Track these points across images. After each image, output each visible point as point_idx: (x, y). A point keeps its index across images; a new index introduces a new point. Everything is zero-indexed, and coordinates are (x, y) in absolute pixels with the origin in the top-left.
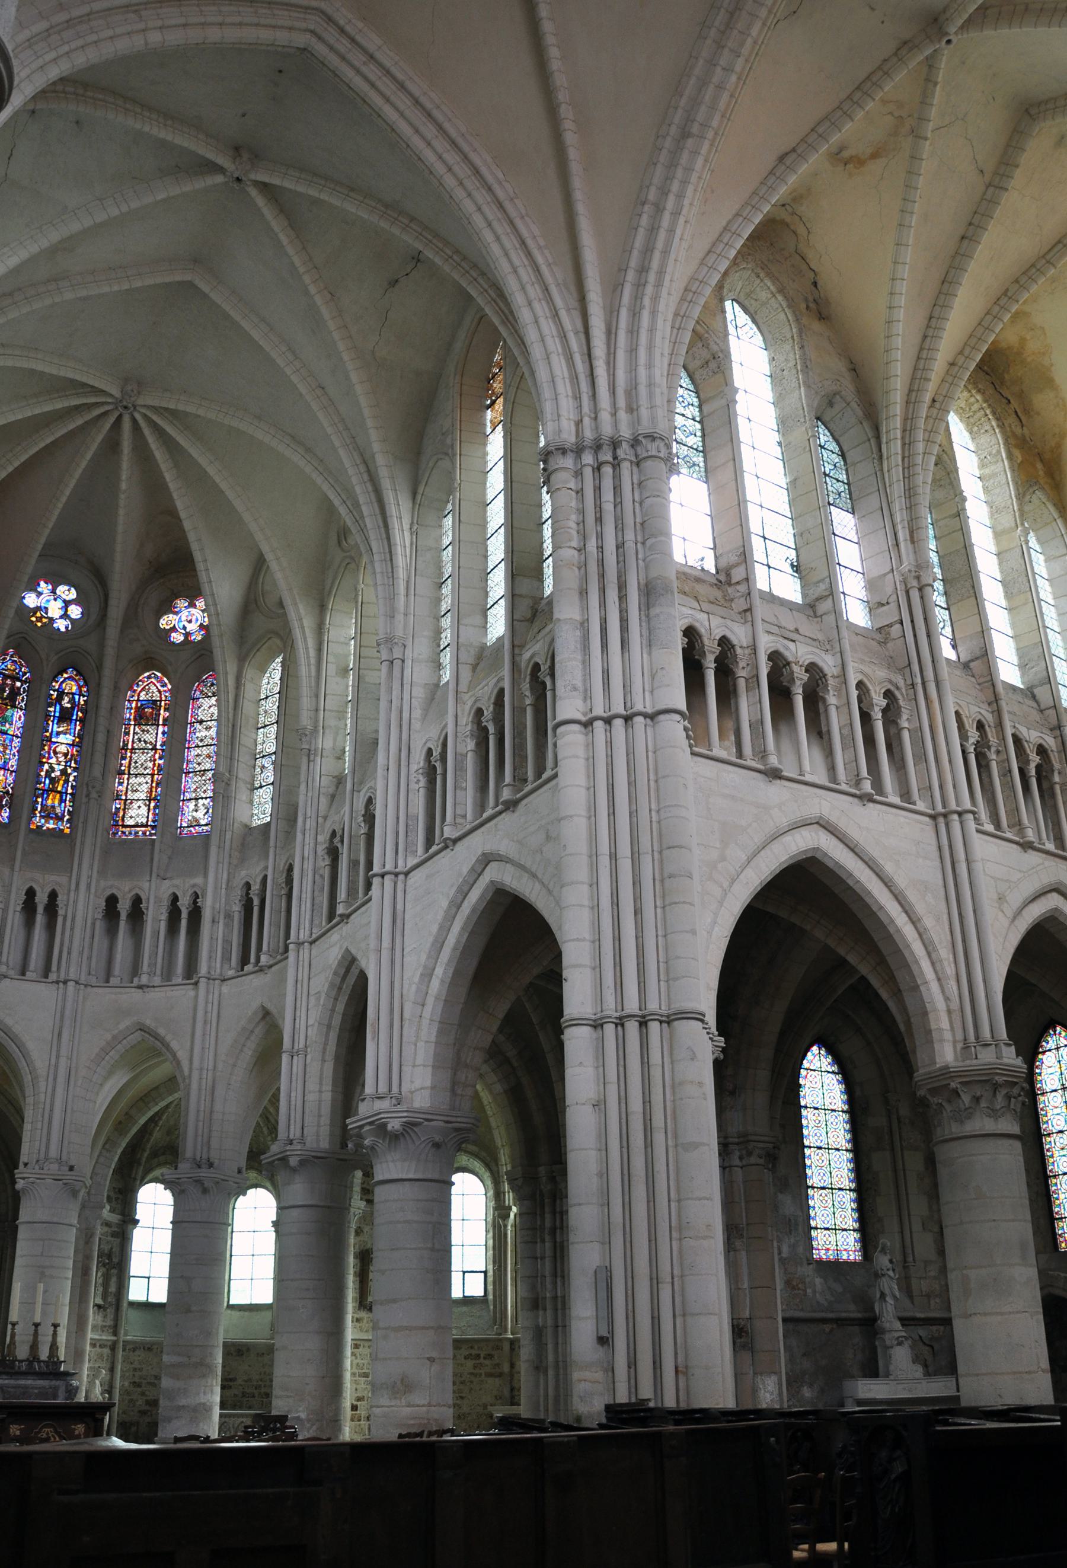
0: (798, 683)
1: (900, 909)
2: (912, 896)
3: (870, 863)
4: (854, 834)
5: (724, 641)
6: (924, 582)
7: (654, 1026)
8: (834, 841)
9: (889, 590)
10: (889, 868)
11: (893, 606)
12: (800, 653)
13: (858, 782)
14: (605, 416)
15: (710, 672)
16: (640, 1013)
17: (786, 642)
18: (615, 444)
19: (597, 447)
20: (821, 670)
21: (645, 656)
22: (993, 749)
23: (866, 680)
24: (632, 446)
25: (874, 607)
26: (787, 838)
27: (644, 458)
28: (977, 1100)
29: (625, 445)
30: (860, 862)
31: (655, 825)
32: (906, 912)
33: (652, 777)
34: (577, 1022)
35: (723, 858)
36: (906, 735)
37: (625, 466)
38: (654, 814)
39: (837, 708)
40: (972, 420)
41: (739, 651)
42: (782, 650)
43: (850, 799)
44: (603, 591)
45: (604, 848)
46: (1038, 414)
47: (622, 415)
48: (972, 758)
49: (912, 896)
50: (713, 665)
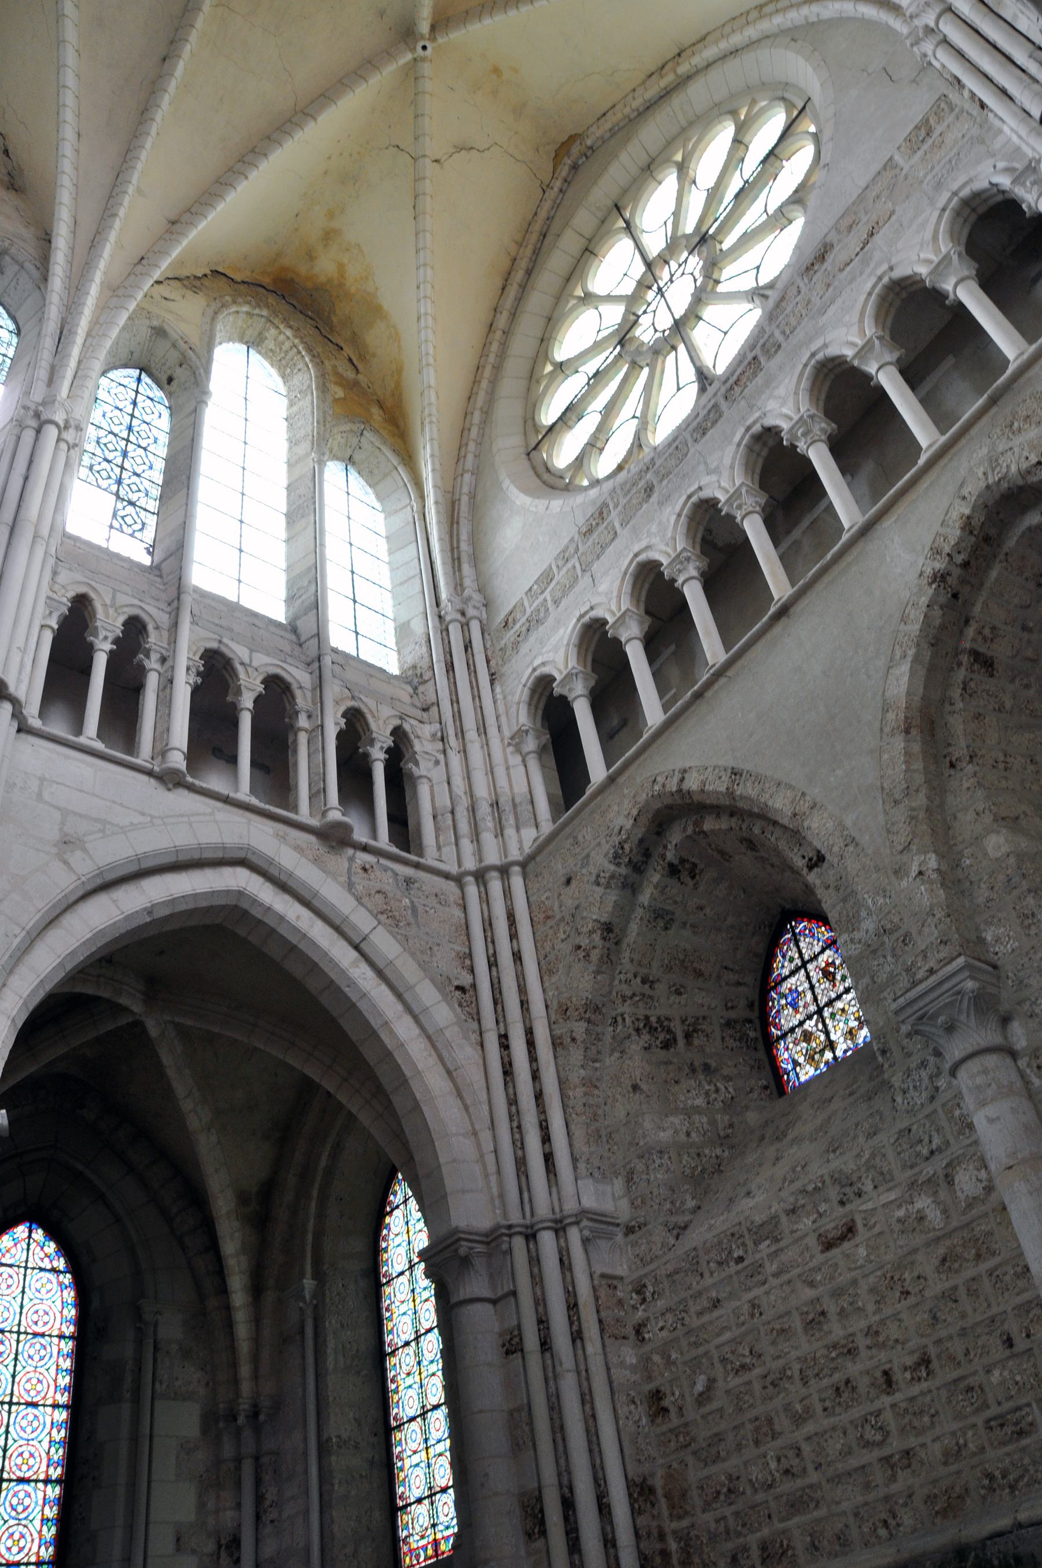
6: (44, 417)
40: (284, 362)
46: (374, 355)
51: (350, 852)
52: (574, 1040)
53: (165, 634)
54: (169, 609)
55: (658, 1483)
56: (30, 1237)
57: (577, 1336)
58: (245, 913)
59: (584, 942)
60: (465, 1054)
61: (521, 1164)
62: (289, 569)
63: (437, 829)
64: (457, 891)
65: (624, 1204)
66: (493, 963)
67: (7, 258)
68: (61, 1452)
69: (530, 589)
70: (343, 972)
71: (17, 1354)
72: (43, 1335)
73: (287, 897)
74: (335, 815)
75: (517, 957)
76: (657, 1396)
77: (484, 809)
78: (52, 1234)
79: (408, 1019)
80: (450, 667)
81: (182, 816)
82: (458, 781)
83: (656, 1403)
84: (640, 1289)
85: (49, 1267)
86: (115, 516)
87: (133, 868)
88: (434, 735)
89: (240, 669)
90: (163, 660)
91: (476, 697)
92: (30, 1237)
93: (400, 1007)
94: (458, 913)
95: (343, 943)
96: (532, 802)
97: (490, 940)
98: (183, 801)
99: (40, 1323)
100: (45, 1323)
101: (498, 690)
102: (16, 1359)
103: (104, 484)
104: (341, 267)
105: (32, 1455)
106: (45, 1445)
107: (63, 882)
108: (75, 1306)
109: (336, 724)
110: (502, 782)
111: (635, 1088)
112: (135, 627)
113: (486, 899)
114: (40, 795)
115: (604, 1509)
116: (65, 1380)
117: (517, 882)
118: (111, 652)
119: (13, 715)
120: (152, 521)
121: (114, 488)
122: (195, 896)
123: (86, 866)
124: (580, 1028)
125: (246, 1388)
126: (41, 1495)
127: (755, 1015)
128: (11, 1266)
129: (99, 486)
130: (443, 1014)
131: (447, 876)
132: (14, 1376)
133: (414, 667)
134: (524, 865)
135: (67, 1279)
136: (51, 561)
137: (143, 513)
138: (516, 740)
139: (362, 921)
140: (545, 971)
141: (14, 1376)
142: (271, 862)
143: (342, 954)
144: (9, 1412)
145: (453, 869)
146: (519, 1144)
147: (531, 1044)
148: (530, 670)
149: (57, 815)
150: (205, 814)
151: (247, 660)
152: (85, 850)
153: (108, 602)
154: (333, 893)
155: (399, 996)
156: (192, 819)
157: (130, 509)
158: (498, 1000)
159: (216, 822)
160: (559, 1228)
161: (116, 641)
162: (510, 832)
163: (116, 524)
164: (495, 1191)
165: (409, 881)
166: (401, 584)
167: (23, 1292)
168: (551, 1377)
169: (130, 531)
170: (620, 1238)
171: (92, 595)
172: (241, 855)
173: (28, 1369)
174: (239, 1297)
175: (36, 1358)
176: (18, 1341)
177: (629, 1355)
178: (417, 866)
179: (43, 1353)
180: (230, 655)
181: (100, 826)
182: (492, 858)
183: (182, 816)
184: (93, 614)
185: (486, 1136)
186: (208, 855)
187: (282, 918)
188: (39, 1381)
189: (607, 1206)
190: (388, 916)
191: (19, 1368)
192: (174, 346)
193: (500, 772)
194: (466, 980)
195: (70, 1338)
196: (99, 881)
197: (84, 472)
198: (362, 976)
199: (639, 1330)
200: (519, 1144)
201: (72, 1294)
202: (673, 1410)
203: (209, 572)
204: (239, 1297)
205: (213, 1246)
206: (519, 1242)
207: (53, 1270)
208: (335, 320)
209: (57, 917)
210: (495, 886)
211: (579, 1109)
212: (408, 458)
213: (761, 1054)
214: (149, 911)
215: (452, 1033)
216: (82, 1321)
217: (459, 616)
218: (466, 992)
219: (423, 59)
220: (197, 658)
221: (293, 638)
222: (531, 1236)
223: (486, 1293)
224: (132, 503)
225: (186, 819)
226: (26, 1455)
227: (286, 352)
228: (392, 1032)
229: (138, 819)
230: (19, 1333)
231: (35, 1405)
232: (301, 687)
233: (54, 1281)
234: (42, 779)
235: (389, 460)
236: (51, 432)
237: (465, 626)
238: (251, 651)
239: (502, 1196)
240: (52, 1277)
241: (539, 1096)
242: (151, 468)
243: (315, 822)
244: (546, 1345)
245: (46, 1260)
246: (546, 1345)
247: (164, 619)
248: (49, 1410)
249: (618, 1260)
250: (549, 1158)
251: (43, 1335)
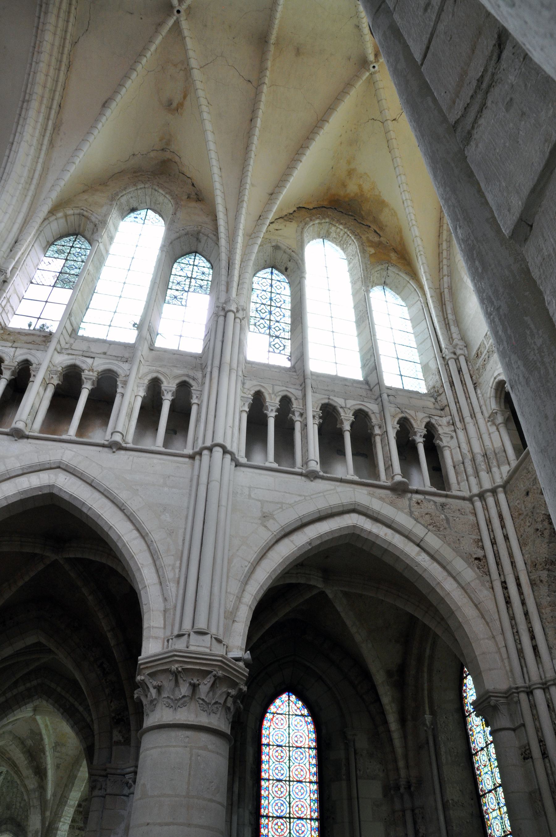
3: (105, 493)
4: (93, 472)
10: (123, 496)
28: (159, 689)
30: (97, 495)
32: (138, 530)
40: (342, 242)
46: (386, 226)
49: (143, 517)
51: (409, 495)
52: (541, 581)
53: (301, 401)
54: (301, 388)
56: (289, 700)
58: (359, 536)
59: (540, 526)
60: (484, 595)
61: (520, 652)
62: (361, 350)
63: (457, 473)
64: (471, 506)
66: (494, 543)
67: (201, 234)
68: (316, 805)
69: (486, 335)
70: (413, 560)
71: (289, 757)
72: (301, 747)
73: (379, 525)
74: (398, 478)
75: (506, 538)
77: (479, 459)
78: (300, 697)
79: (450, 580)
80: (452, 384)
81: (319, 493)
82: (464, 446)
85: (300, 714)
86: (270, 346)
87: (299, 523)
88: (448, 423)
89: (341, 410)
90: (301, 415)
91: (468, 398)
92: (289, 700)
93: (445, 574)
94: (472, 518)
95: (411, 544)
96: (505, 451)
97: (491, 530)
98: (319, 485)
99: (299, 742)
100: (301, 742)
101: (479, 392)
102: (289, 760)
103: (262, 331)
104: (360, 186)
105: (302, 806)
106: (308, 801)
107: (265, 536)
108: (315, 733)
109: (394, 428)
110: (487, 442)
112: (286, 401)
113: (486, 508)
114: (250, 495)
116: (314, 770)
117: (502, 497)
118: (276, 416)
119: (232, 460)
120: (288, 343)
121: (268, 332)
122: (332, 532)
123: (275, 527)
124: (544, 575)
125: (403, 773)
126: (309, 826)
128: (282, 714)
129: (260, 333)
130: (469, 574)
131: (464, 499)
132: (289, 768)
133: (434, 387)
134: (504, 487)
135: (309, 719)
136: (240, 379)
137: (283, 340)
138: (492, 418)
139: (419, 531)
140: (522, 544)
141: (289, 768)
142: (368, 508)
143: (411, 550)
144: (289, 785)
145: (467, 494)
146: (518, 641)
147: (519, 585)
148: (493, 379)
149: (259, 504)
150: (331, 490)
151: (343, 405)
152: (274, 519)
153: (271, 392)
154: (402, 519)
155: (444, 568)
156: (325, 493)
157: (277, 340)
158: (498, 563)
159: (337, 493)
161: (278, 410)
162: (495, 469)
163: (271, 350)
164: (508, 668)
165: (443, 505)
166: (421, 343)
167: (289, 727)
169: (278, 351)
171: (263, 390)
172: (352, 507)
173: (296, 764)
174: (394, 726)
175: (299, 759)
176: (289, 751)
178: (446, 496)
179: (302, 756)
180: (335, 404)
181: (280, 506)
182: (487, 485)
183: (319, 493)
184: (265, 399)
185: (500, 638)
186: (335, 510)
187: (377, 536)
188: (302, 770)
190: (433, 526)
191: (291, 764)
192: (285, 252)
193: (485, 437)
194: (480, 554)
195: (314, 748)
196: (283, 533)
197: (252, 327)
198: (423, 560)
200: (518, 641)
201: (313, 726)
203: (319, 363)
204: (394, 726)
205: (378, 700)
206: (523, 697)
207: (302, 715)
208: (363, 213)
209: (265, 554)
210: (490, 500)
211: (549, 619)
212: (414, 275)
214: (310, 543)
215: (475, 584)
216: (319, 739)
217: (453, 356)
219: (375, 73)
220: (318, 410)
221: (367, 387)
222: (530, 693)
223: (508, 725)
224: (277, 337)
225: (322, 494)
226: (300, 806)
227: (342, 237)
228: (442, 588)
229: (298, 498)
230: (289, 747)
231: (301, 782)
232: (374, 413)
233: (303, 721)
234: (250, 488)
235: (404, 279)
236: (231, 316)
237: (457, 360)
238: (345, 400)
239: (511, 671)
240: (302, 718)
241: (526, 614)
242: (284, 316)
243: (389, 484)
245: (298, 710)
247: (299, 394)
248: (308, 784)
250: (535, 648)
251: (301, 747)
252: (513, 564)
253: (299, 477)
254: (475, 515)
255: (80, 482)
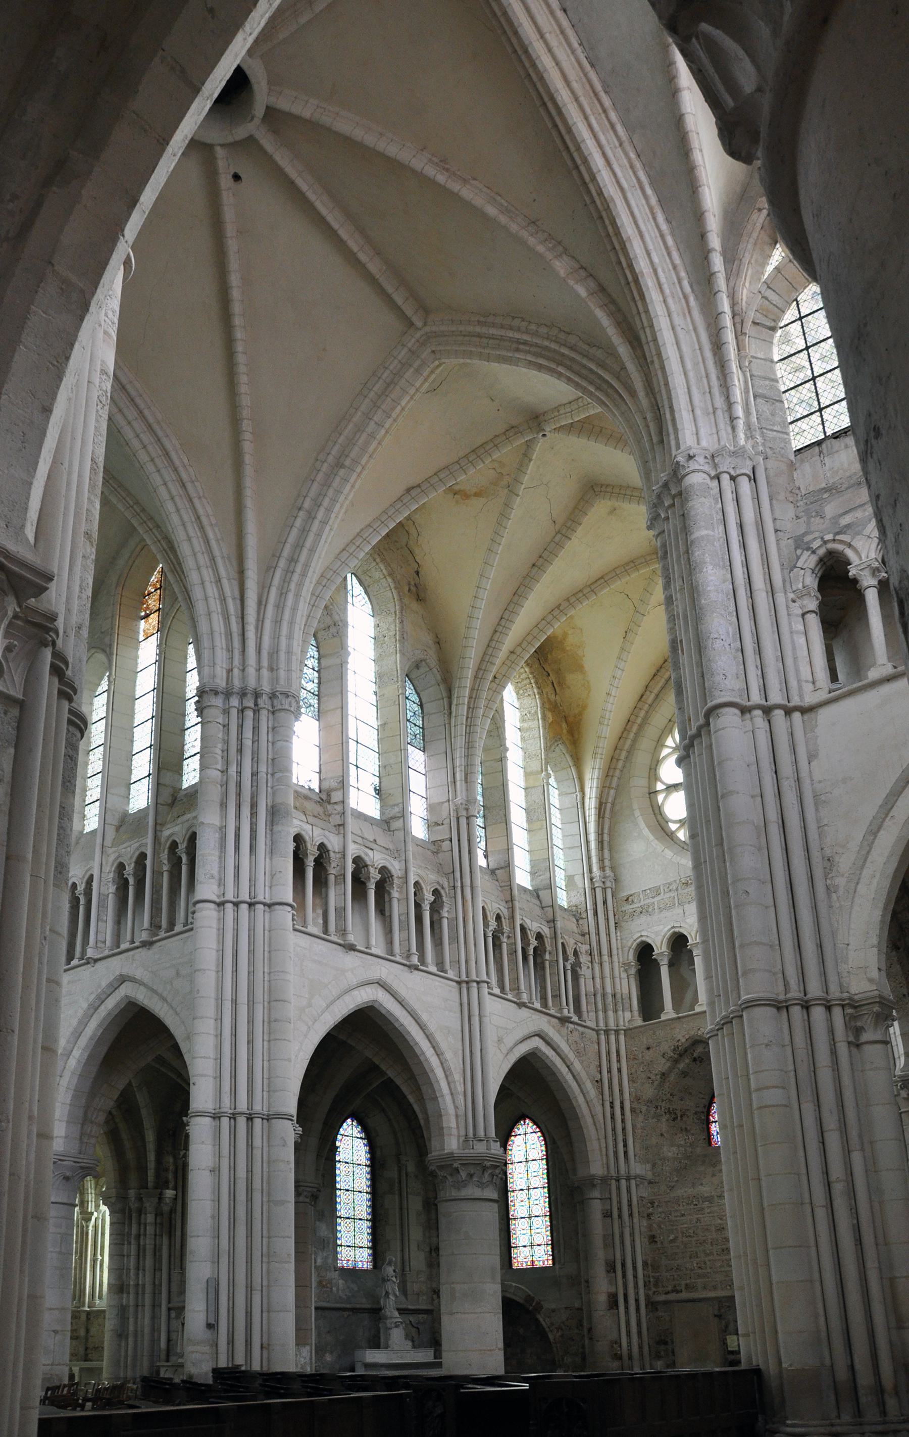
0: (373, 881)
1: (429, 1045)
2: (439, 1037)
4: (403, 992)
5: (322, 847)
7: (258, 1122)
8: (388, 996)
9: (445, 814)
10: (425, 1017)
11: (446, 827)
12: (376, 859)
13: (409, 956)
14: (251, 671)
15: (311, 868)
16: (248, 1112)
17: (367, 850)
18: (257, 695)
19: (243, 694)
20: (389, 872)
21: (267, 860)
22: (505, 935)
23: (421, 882)
24: (270, 698)
25: (431, 825)
26: (356, 992)
27: (279, 710)
29: (265, 697)
30: (405, 1012)
31: (266, 983)
32: (434, 1048)
33: (266, 949)
34: (202, 1114)
35: (310, 1005)
36: (445, 922)
37: (264, 713)
38: (266, 975)
39: (399, 900)
41: (332, 855)
42: (363, 856)
43: (402, 967)
44: (239, 806)
45: (228, 995)
47: (265, 673)
48: (490, 940)
50: (312, 864)
55: (649, 1262)
57: (631, 1215)
61: (616, 1153)
65: (650, 1173)
66: (609, 1071)
75: (619, 1070)
76: (653, 1237)
80: (596, 913)
83: (652, 1239)
84: (652, 1203)
88: (586, 952)
91: (608, 935)
98: (525, 1012)
101: (618, 934)
110: (618, 987)
111: (662, 1135)
113: (608, 1042)
115: (635, 1268)
127: (705, 1110)
130: (592, 1093)
131: (593, 1030)
138: (626, 966)
139: (571, 1056)
140: (632, 1080)
143: (564, 1069)
160: (628, 1179)
162: (620, 1013)
164: (605, 1161)
165: (583, 1033)
166: (569, 848)
168: (622, 1226)
170: (646, 1184)
177: (645, 1223)
185: (603, 1141)
189: (643, 1173)
190: (578, 1053)
198: (569, 1077)
199: (649, 1215)
202: (659, 1243)
206: (613, 1182)
210: (612, 1038)
212: (577, 761)
213: (705, 1126)
215: (595, 1101)
217: (601, 885)
218: (599, 1082)
221: (538, 903)
222: (618, 1180)
237: (604, 890)
239: (607, 1164)
241: (624, 1129)
244: (620, 1216)
246: (620, 1216)
249: (645, 1192)
250: (626, 1153)
252: (621, 1091)
253: (513, 1004)
254: (598, 1044)
255: (392, 999)
